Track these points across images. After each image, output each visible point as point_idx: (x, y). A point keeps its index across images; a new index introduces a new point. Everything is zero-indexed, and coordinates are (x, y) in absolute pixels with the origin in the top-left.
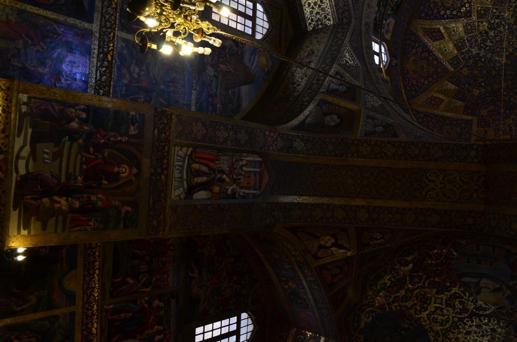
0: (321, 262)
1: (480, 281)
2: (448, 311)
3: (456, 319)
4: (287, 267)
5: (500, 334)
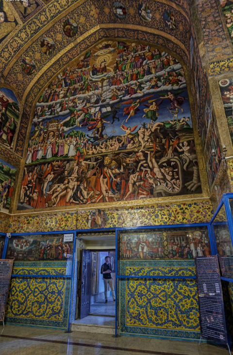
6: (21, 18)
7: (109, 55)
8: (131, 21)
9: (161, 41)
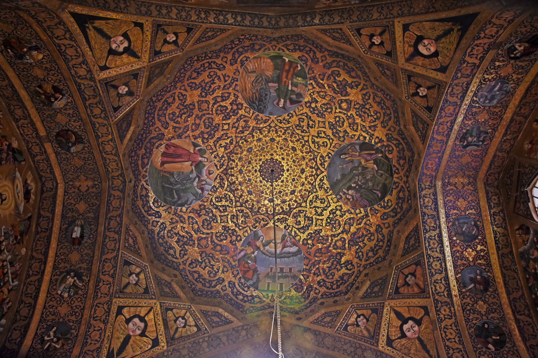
0: (422, 302)
1: (282, 250)
2: (311, 213)
3: (304, 204)
4: (470, 287)
5: (266, 198)
6: (106, 79)
7: (13, 206)
8: (62, 251)
9: (24, 312)
